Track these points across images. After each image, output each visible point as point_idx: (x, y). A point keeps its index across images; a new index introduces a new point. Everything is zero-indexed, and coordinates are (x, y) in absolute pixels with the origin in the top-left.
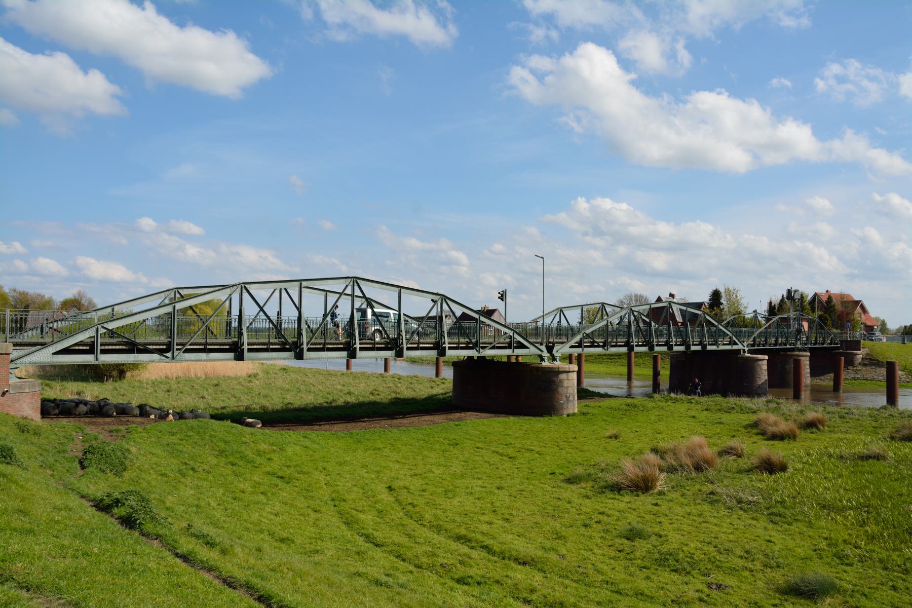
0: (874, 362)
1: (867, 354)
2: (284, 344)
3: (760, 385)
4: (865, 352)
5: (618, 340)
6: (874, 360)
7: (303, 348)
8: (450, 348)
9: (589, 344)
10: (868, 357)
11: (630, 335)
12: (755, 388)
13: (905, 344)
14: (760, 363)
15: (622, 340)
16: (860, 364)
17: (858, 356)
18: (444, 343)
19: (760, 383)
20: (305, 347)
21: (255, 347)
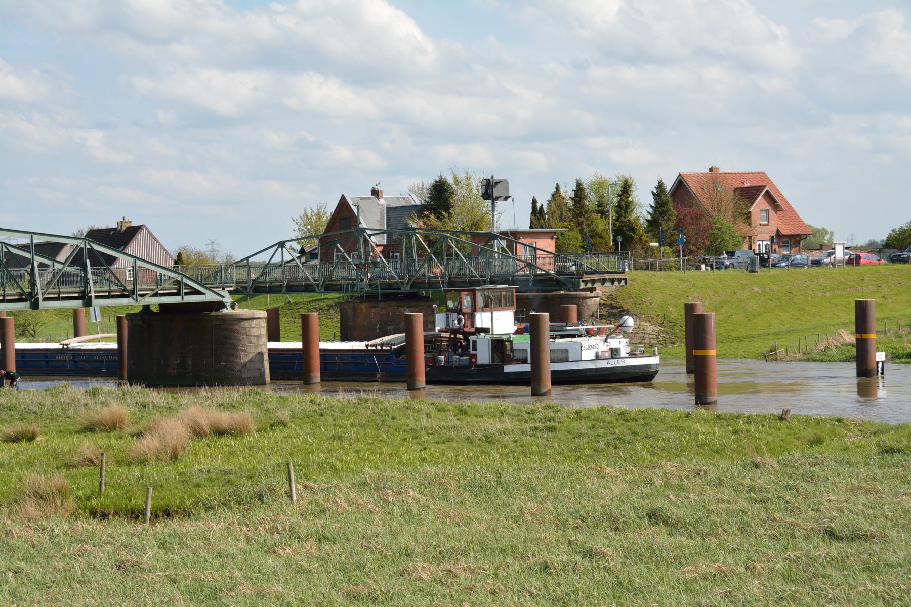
0: (615, 311)
1: (610, 297)
2: (22, 294)
3: (246, 363)
4: (608, 294)
5: (61, 290)
6: (616, 307)
7: (38, 298)
8: (97, 297)
9: (16, 298)
10: (608, 303)
11: (86, 283)
12: (236, 370)
13: (754, 271)
14: (246, 324)
15: (74, 290)
16: (592, 315)
17: (589, 302)
18: (90, 292)
19: (247, 360)
20: (40, 297)
21: (101, 294)
